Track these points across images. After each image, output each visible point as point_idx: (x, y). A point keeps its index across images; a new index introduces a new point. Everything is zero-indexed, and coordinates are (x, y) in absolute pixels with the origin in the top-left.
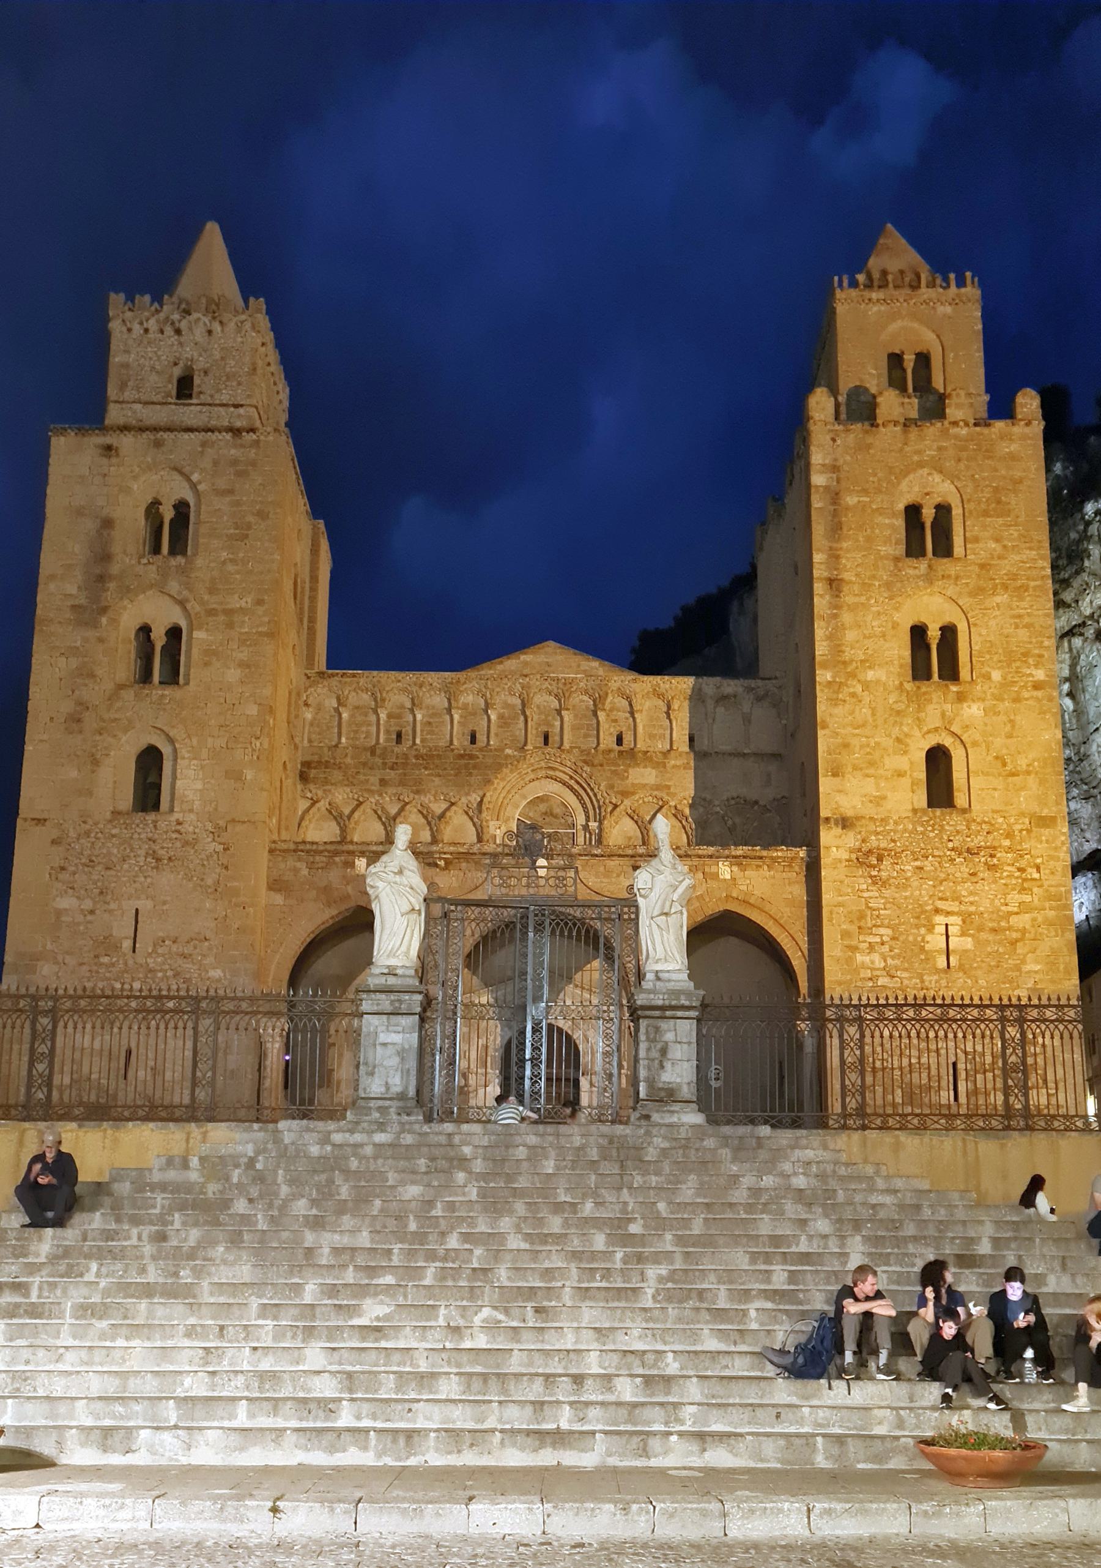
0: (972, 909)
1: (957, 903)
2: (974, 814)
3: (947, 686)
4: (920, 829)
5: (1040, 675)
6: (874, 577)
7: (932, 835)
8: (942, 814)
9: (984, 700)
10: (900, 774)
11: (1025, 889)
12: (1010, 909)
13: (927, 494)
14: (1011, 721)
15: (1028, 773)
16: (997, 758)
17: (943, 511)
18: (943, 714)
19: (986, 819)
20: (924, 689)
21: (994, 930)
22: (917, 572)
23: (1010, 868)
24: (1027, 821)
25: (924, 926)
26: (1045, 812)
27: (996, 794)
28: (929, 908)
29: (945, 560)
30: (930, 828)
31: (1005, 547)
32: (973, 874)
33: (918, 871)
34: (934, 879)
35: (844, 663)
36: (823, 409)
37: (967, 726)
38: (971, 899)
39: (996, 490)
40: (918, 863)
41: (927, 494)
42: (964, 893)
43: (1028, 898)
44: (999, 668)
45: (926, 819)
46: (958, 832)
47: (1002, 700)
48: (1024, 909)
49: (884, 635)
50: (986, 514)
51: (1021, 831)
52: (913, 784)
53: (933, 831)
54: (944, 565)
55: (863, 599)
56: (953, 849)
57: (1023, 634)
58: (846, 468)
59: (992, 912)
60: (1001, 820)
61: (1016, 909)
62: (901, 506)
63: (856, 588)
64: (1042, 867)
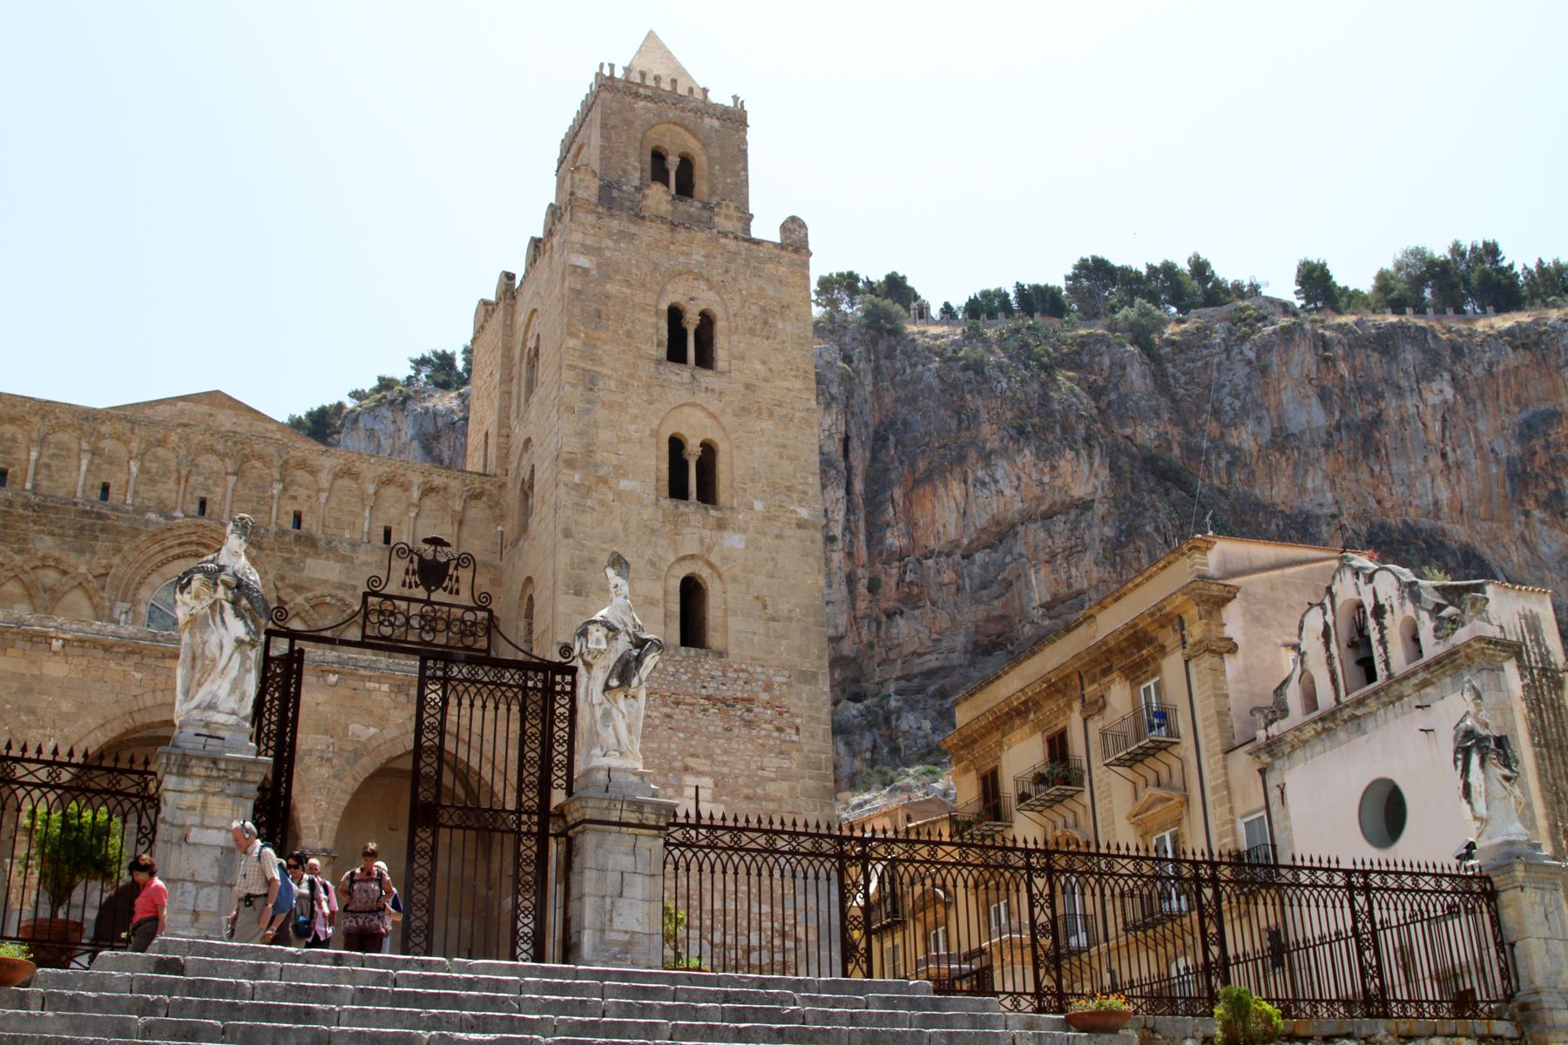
0: (725, 770)
1: (709, 762)
2: (731, 659)
3: (706, 509)
4: (671, 669)
5: (804, 513)
6: (632, 376)
7: (684, 678)
8: (697, 655)
9: (745, 531)
10: (652, 602)
11: (782, 753)
12: (765, 773)
13: (692, 299)
14: (773, 559)
15: (790, 619)
16: (757, 598)
17: (707, 320)
18: (702, 540)
19: (744, 666)
20: (682, 508)
21: (748, 798)
22: (678, 379)
23: (766, 726)
24: (786, 673)
25: (673, 786)
26: (807, 667)
27: (756, 639)
28: (677, 764)
29: (710, 372)
30: (682, 670)
31: (770, 370)
32: (729, 730)
33: (667, 720)
34: (685, 730)
35: (596, 465)
36: (587, 188)
37: (727, 558)
38: (725, 759)
39: (763, 309)
40: (667, 710)
41: (692, 299)
42: (718, 751)
43: (786, 764)
44: (761, 499)
45: (677, 658)
46: (713, 677)
47: (765, 534)
48: (783, 775)
49: (641, 441)
50: (752, 332)
51: (781, 684)
52: (666, 616)
53: (685, 673)
54: (706, 377)
55: (619, 398)
56: (708, 698)
57: (787, 466)
58: (608, 254)
59: (748, 776)
60: (759, 670)
61: (773, 775)
62: (664, 306)
63: (613, 384)
64: (802, 729)
